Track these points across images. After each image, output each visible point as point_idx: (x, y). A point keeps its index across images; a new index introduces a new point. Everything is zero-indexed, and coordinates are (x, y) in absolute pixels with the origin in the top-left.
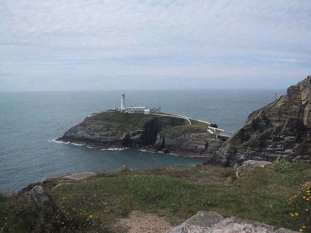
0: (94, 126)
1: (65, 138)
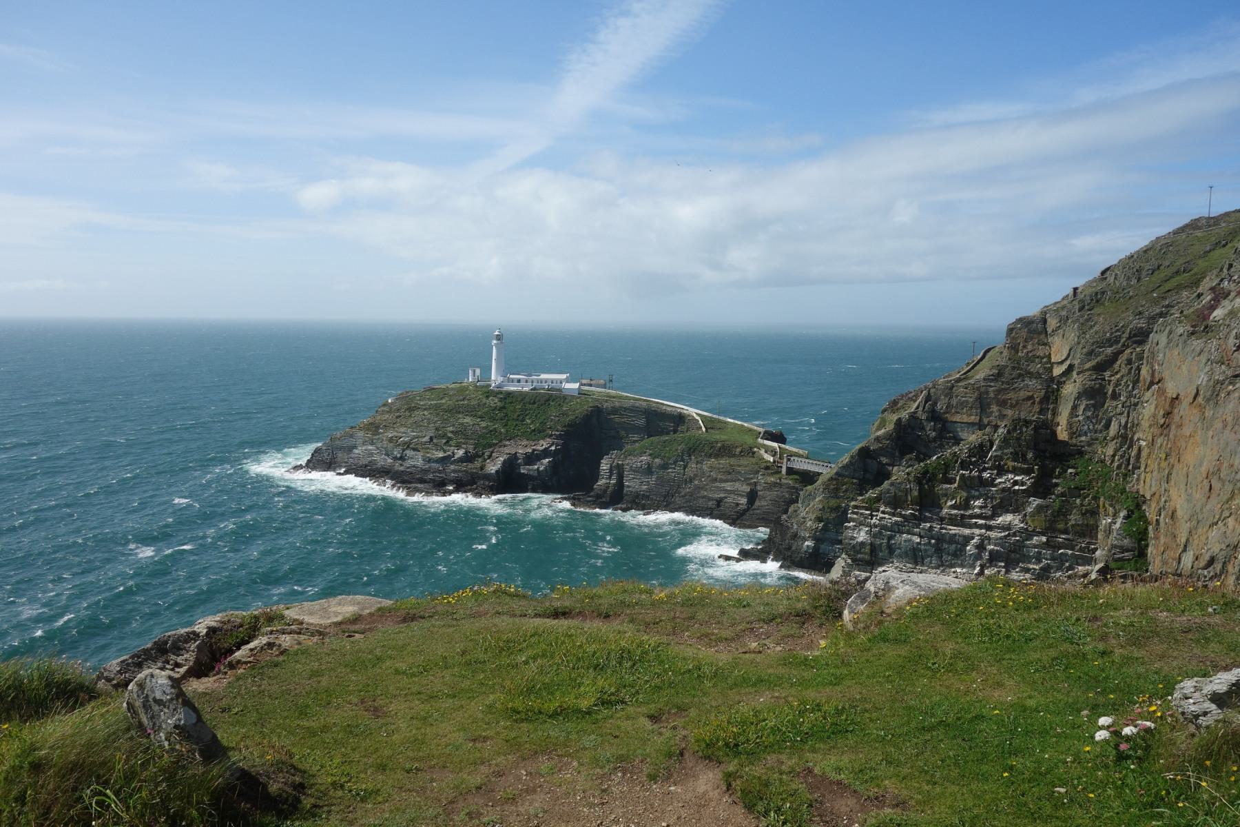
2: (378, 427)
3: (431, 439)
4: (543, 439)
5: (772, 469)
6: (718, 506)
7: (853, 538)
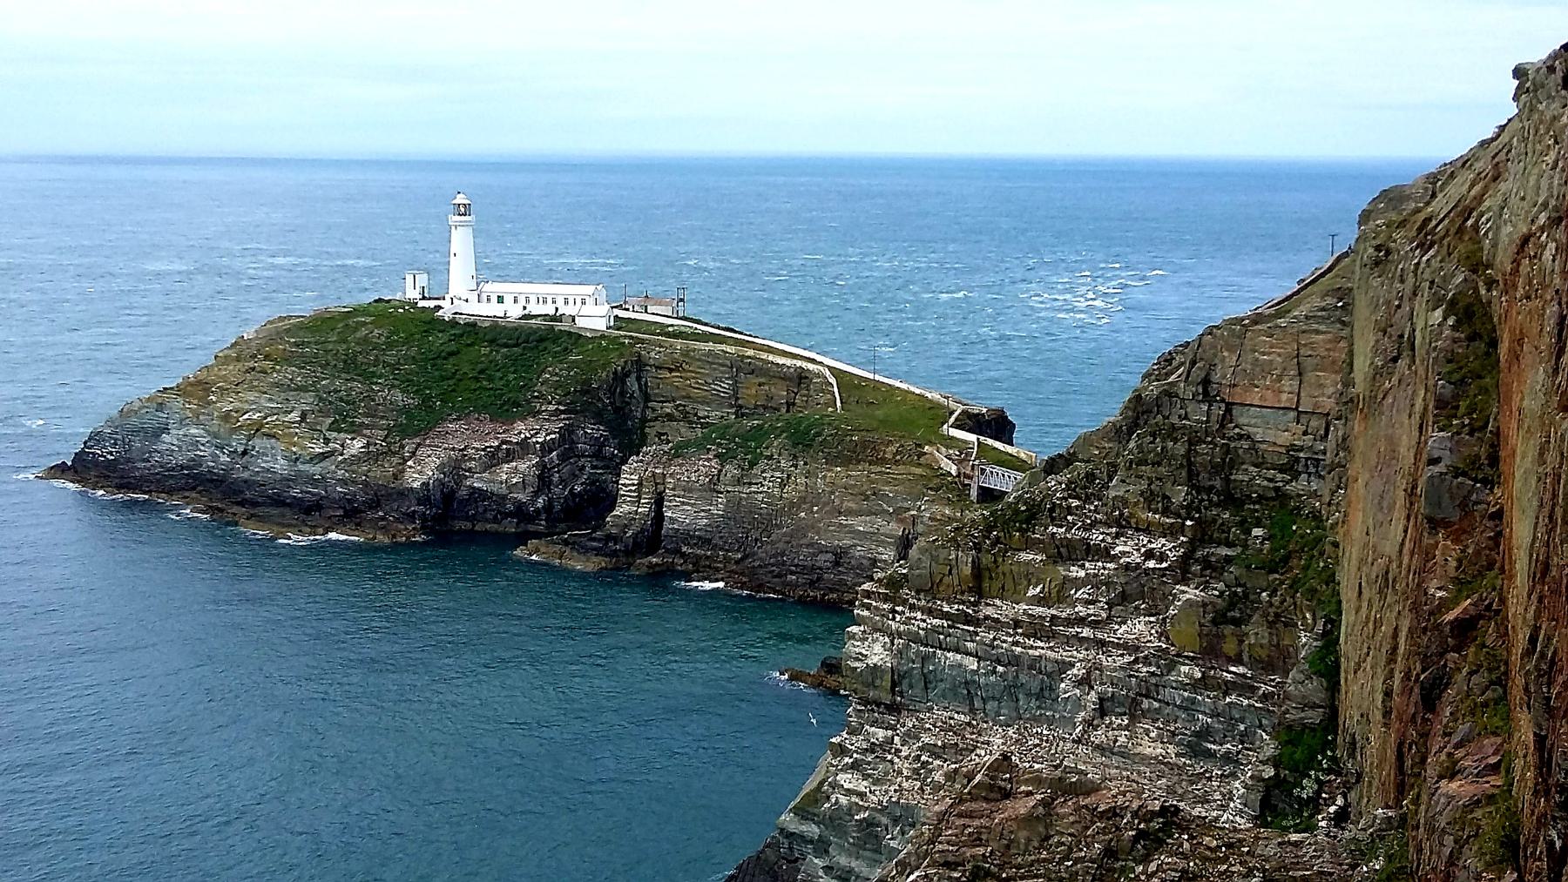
0: (254, 405)
1: (82, 468)
2: (207, 391)
3: (303, 416)
4: (523, 419)
5: (956, 489)
6: (837, 564)
7: (861, 657)
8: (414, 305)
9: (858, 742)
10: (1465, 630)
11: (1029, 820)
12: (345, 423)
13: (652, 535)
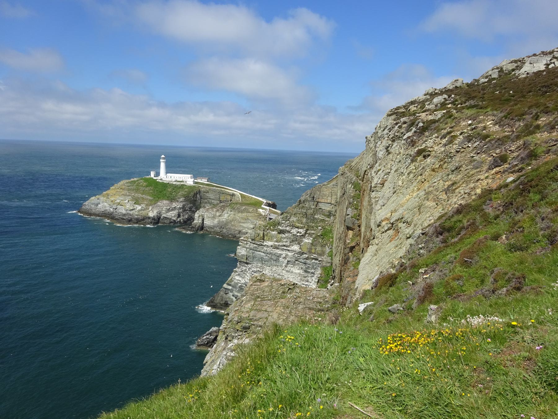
8: (152, 178)
9: (240, 270)
10: (352, 249)
11: (268, 286)
12: (137, 202)
13: (202, 227)
